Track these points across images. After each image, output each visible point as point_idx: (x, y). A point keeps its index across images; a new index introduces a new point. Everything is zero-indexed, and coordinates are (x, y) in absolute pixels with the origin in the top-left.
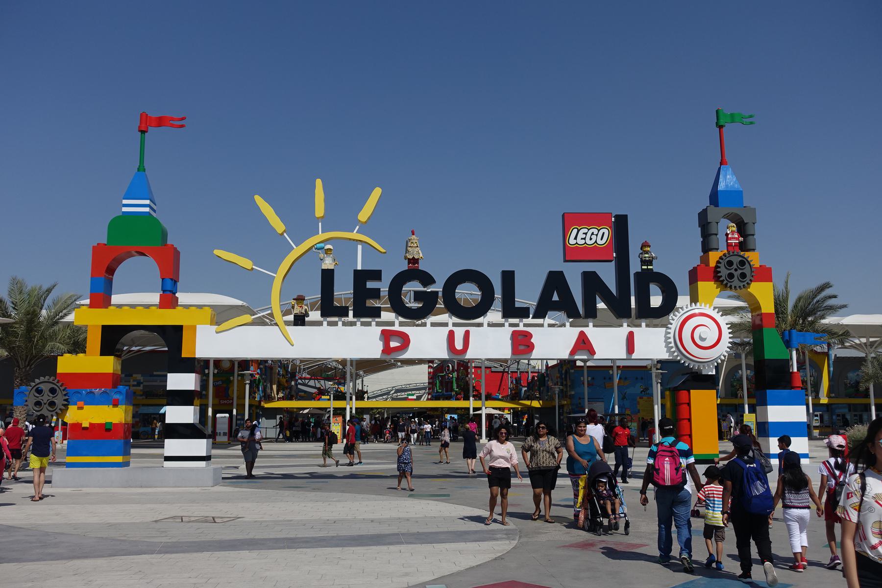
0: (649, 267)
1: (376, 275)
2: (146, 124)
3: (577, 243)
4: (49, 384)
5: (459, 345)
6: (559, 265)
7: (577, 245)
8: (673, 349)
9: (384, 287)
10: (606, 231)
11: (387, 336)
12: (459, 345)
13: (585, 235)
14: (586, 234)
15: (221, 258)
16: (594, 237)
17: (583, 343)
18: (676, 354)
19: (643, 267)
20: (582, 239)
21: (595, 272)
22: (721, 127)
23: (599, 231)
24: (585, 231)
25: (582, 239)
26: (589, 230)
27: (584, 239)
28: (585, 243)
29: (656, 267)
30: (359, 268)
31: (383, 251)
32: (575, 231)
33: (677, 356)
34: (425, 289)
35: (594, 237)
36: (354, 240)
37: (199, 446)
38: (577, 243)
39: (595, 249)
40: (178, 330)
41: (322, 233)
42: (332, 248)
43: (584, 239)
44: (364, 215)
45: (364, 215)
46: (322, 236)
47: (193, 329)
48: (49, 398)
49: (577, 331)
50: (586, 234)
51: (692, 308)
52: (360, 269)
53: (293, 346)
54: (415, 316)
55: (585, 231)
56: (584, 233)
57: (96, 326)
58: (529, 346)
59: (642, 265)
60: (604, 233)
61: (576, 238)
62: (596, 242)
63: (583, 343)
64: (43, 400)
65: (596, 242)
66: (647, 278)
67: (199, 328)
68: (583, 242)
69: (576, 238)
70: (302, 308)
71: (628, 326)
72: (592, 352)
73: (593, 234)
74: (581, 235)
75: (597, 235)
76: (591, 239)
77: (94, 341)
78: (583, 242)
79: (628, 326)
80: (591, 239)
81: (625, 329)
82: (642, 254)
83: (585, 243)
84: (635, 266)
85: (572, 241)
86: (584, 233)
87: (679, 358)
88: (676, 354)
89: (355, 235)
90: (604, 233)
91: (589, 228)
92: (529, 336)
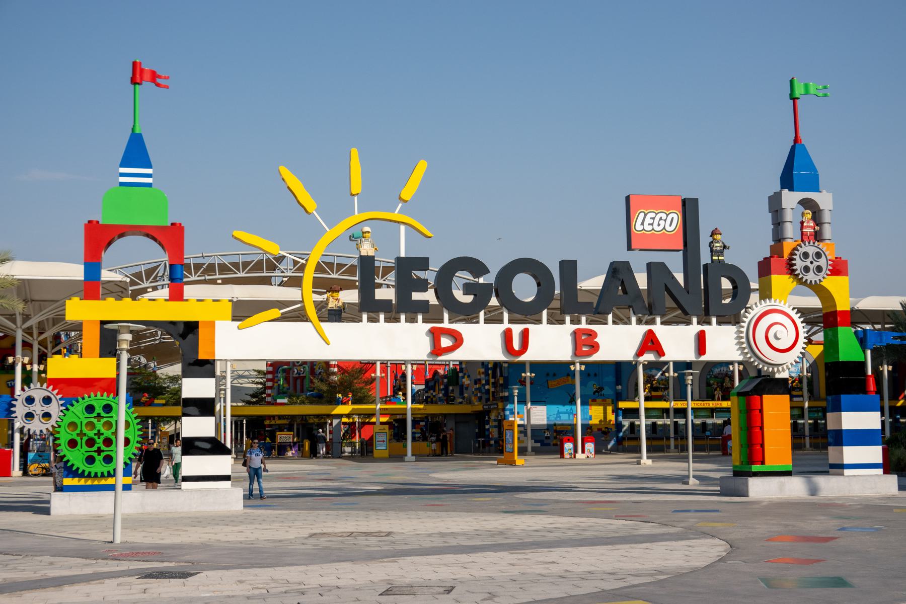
0: (720, 258)
1: (423, 263)
2: (137, 75)
3: (644, 229)
4: (46, 392)
5: (516, 345)
6: (623, 255)
7: (643, 231)
8: (746, 351)
9: (430, 276)
10: (675, 216)
11: (435, 335)
12: (516, 345)
13: (652, 220)
14: (653, 219)
15: (242, 241)
16: (662, 222)
17: (650, 343)
18: (749, 355)
19: (714, 258)
20: (649, 224)
21: (663, 263)
22: (794, 100)
23: (667, 215)
24: (653, 215)
25: (649, 224)
26: (656, 214)
27: (652, 224)
28: (653, 229)
29: (728, 258)
30: (403, 255)
31: (429, 234)
32: (642, 215)
33: (750, 358)
34: (476, 280)
35: (662, 222)
36: (395, 222)
37: (222, 464)
38: (644, 229)
39: (664, 235)
40: (191, 327)
41: (358, 213)
42: (370, 230)
43: (652, 224)
44: (408, 193)
45: (408, 193)
46: (358, 217)
47: (212, 325)
48: (43, 408)
49: (645, 328)
50: (653, 219)
51: (775, 304)
52: (404, 256)
53: (328, 344)
54: (467, 314)
55: (653, 215)
56: (651, 218)
57: (93, 322)
58: (593, 347)
59: (712, 256)
60: (673, 218)
61: (642, 224)
62: (664, 228)
63: (650, 343)
64: (34, 411)
65: (664, 228)
66: (720, 268)
67: (218, 324)
68: (650, 228)
69: (642, 224)
70: (339, 302)
71: (699, 323)
72: (661, 353)
73: (661, 219)
74: (648, 220)
75: (665, 220)
76: (659, 225)
77: (91, 339)
78: (650, 228)
79: (699, 323)
80: (659, 225)
81: (695, 328)
82: (712, 242)
83: (653, 229)
84: (705, 258)
85: (639, 227)
86: (651, 218)
87: (752, 360)
88: (749, 355)
89: (396, 215)
90: (673, 218)
91: (657, 212)
92: (592, 334)
